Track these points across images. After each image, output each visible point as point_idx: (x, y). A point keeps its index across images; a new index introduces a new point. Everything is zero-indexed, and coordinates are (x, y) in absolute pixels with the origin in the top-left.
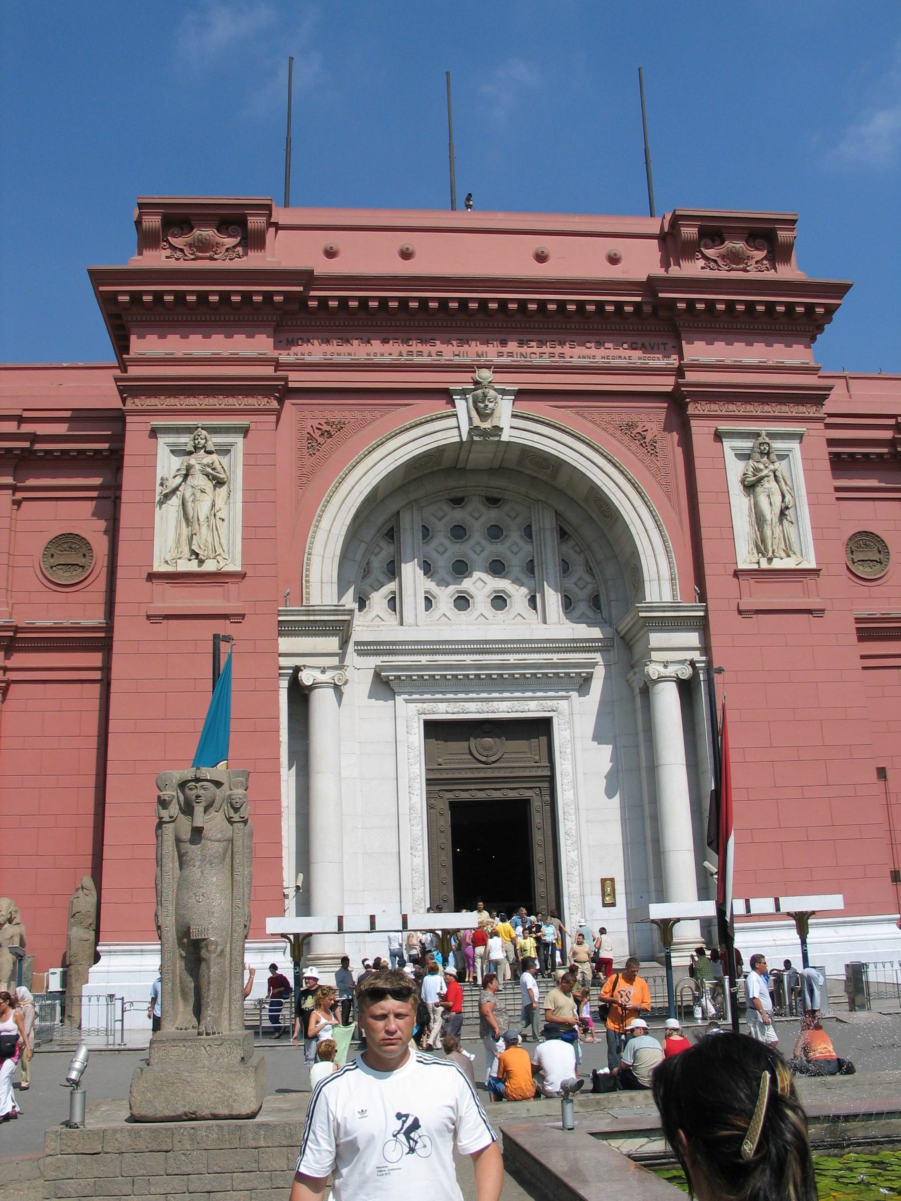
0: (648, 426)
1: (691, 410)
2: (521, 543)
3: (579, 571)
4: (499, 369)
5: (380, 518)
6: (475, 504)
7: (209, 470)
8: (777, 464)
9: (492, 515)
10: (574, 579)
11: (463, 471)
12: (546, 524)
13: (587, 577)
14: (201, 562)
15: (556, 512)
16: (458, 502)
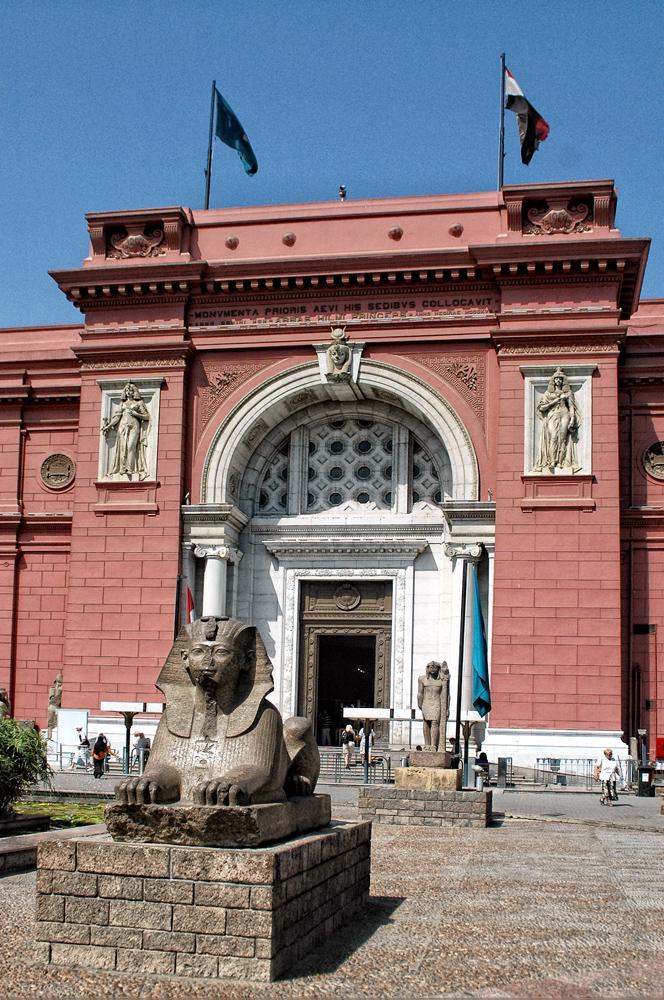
0: (470, 366)
1: (500, 353)
2: (384, 454)
3: (427, 475)
4: (350, 328)
5: (275, 440)
6: (351, 426)
7: (135, 413)
8: (569, 393)
9: (364, 434)
10: (422, 480)
11: (337, 403)
12: (401, 438)
13: (432, 479)
14: (130, 476)
15: (410, 431)
16: (337, 425)
